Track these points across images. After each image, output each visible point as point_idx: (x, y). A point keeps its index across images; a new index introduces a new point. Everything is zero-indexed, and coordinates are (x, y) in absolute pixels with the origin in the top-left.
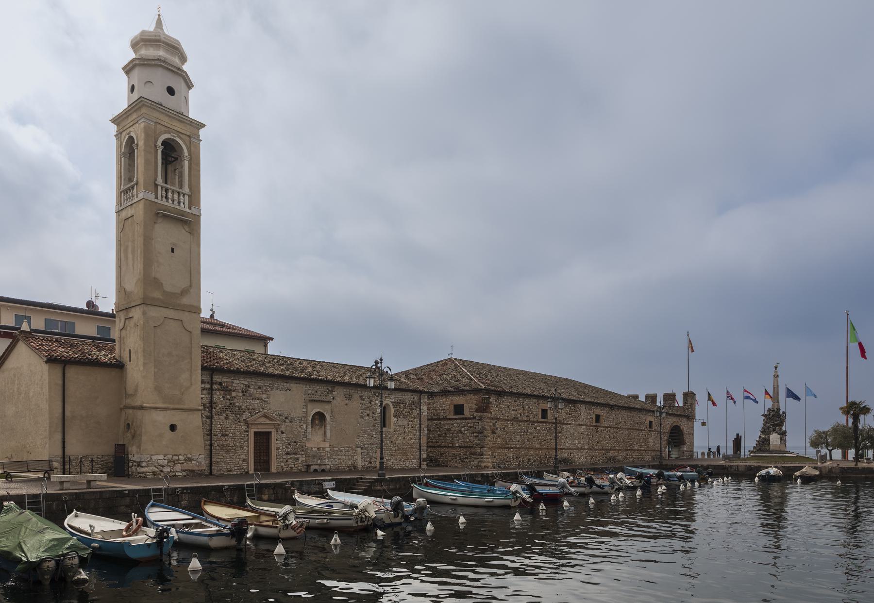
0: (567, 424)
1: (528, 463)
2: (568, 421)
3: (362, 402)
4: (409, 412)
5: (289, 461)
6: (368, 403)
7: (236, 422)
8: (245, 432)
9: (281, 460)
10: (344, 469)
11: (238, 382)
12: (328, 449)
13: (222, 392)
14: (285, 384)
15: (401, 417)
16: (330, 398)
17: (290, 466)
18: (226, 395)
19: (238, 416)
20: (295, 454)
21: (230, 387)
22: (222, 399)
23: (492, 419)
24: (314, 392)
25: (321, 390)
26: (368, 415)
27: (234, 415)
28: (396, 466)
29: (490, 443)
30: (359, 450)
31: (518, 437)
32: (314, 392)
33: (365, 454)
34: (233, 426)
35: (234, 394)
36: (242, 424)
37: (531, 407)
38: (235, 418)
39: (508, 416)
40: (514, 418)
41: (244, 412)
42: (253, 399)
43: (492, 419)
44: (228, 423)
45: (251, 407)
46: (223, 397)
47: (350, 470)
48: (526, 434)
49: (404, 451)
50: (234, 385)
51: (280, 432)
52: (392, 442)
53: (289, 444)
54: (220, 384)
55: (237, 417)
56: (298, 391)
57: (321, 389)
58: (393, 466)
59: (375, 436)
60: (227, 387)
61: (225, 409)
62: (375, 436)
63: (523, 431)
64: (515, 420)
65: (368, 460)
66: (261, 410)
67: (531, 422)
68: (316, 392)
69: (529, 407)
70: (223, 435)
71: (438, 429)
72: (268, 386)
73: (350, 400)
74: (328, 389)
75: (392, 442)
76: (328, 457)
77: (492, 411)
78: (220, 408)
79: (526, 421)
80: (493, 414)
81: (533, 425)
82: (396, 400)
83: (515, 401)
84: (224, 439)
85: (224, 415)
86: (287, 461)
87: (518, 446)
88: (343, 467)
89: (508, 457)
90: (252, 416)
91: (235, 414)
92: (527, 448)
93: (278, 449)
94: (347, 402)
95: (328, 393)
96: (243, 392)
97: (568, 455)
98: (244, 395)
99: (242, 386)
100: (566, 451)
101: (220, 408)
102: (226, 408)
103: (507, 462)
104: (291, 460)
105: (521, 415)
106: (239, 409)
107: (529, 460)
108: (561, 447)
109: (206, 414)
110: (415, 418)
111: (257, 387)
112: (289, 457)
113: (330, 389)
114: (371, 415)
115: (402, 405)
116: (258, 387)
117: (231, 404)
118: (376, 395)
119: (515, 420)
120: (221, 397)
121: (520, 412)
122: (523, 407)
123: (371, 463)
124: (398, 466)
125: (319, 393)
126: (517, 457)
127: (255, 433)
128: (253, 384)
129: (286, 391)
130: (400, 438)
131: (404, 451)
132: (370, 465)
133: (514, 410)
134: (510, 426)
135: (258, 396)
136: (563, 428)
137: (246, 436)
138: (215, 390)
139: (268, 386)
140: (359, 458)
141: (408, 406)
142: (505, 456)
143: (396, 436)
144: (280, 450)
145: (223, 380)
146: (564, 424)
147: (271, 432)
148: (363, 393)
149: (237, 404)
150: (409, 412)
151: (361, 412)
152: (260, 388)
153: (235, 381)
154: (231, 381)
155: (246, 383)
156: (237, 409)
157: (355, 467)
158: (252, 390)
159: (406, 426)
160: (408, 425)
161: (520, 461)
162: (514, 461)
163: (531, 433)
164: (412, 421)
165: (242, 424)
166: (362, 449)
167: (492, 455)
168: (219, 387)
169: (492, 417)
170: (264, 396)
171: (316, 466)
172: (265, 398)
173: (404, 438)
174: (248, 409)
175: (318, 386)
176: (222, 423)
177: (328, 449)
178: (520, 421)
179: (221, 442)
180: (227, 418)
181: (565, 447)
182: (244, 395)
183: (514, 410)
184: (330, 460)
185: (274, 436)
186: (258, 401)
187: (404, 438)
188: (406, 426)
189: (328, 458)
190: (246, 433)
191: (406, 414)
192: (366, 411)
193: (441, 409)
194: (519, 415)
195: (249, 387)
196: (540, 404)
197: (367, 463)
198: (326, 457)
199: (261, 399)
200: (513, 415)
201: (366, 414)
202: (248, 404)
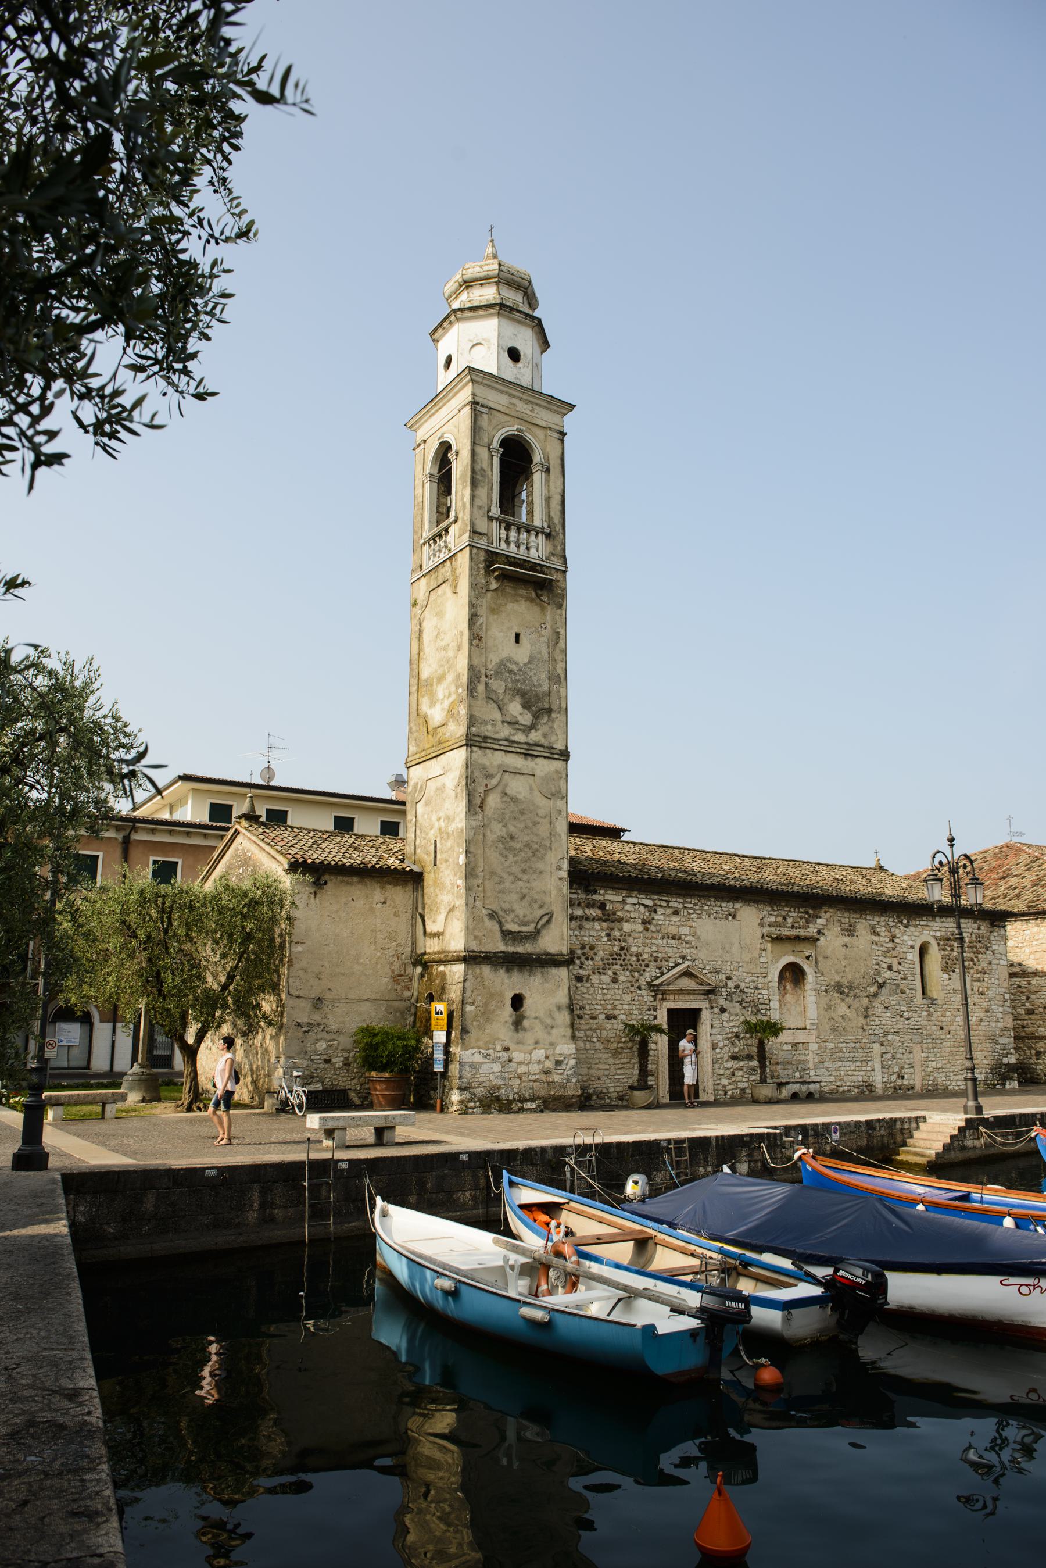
3: (875, 938)
4: (972, 960)
6: (887, 940)
7: (632, 989)
8: (649, 1010)
9: (722, 1072)
10: (849, 1091)
11: (635, 901)
12: (814, 1047)
13: (605, 924)
14: (724, 905)
16: (811, 931)
17: (740, 1085)
18: (612, 929)
19: (636, 974)
21: (619, 913)
22: (605, 939)
24: (780, 919)
25: (794, 914)
26: (890, 968)
27: (628, 973)
28: (954, 1083)
30: (876, 1046)
33: (889, 1056)
34: (627, 997)
35: (627, 927)
36: (644, 992)
38: (630, 979)
41: (647, 966)
42: (663, 938)
44: (617, 990)
45: (660, 955)
46: (608, 935)
47: (862, 1092)
50: (627, 908)
51: (716, 1010)
52: (942, 1028)
53: (737, 1036)
55: (633, 977)
59: (906, 1014)
60: (614, 913)
61: (611, 961)
62: (906, 1014)
65: (896, 1069)
66: (680, 961)
68: (785, 919)
70: (608, 1017)
71: (1024, 998)
72: (690, 908)
74: (807, 913)
75: (942, 1028)
76: (815, 1064)
78: (602, 959)
82: (943, 934)
84: (610, 1026)
85: (610, 973)
86: (733, 1074)
88: (846, 1088)
90: (662, 974)
91: (631, 971)
93: (714, 1047)
94: (846, 939)
95: (807, 922)
98: (647, 929)
99: (642, 909)
101: (602, 959)
102: (615, 957)
104: (741, 1073)
106: (638, 960)
109: (575, 972)
111: (669, 911)
112: (736, 1064)
113: (811, 912)
114: (895, 968)
116: (671, 910)
117: (622, 949)
118: (902, 923)
120: (603, 934)
123: (903, 1077)
125: (790, 920)
127: (670, 1011)
128: (664, 904)
129: (727, 918)
132: (899, 1082)
135: (673, 930)
137: (651, 1018)
138: (593, 919)
139: (690, 908)
140: (878, 1067)
143: (948, 1014)
144: (718, 1050)
145: (607, 897)
147: (700, 1010)
148: (877, 919)
149: (634, 949)
150: (972, 960)
152: (676, 913)
153: (630, 900)
154: (620, 899)
155: (650, 903)
156: (634, 959)
157: (870, 1087)
158: (662, 917)
165: (644, 992)
166: (882, 1045)
168: (599, 913)
170: (684, 931)
171: (795, 1086)
172: (686, 935)
174: (656, 961)
176: (605, 991)
177: (814, 1047)
179: (604, 1034)
180: (615, 980)
182: (647, 929)
184: (820, 1072)
185: (705, 1016)
186: (673, 941)
189: (816, 1067)
190: (652, 1012)
192: (886, 960)
193: (1027, 950)
195: (655, 911)
197: (895, 1077)
198: (811, 1066)
199: (680, 938)
201: (885, 966)
202: (654, 949)
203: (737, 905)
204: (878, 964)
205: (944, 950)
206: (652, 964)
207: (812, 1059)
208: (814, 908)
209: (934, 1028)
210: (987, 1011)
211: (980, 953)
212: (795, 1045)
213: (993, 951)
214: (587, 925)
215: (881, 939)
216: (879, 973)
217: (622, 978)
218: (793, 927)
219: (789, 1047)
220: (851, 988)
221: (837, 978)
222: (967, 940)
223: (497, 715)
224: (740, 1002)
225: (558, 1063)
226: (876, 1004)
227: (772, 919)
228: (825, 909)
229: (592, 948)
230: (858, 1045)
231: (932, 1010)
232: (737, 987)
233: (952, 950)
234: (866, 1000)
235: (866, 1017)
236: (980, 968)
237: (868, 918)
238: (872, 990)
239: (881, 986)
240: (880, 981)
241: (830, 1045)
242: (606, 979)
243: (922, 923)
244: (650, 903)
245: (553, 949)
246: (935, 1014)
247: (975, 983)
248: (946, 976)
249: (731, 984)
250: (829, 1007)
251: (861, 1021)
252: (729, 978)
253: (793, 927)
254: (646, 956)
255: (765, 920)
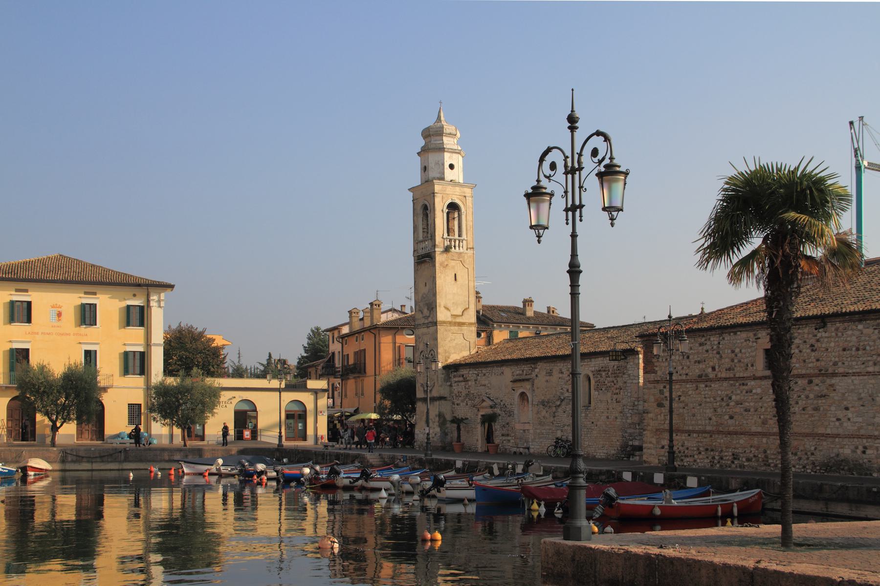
0: (845, 375)
1: (733, 462)
2: (851, 367)
3: (561, 375)
4: (613, 382)
5: (504, 442)
6: (566, 375)
15: (603, 389)
20: (508, 435)
23: (657, 382)
24: (521, 372)
29: (652, 423)
31: (708, 411)
32: (521, 372)
37: (737, 350)
39: (687, 374)
40: (700, 376)
43: (657, 382)
48: (728, 405)
49: (608, 435)
50: (470, 375)
54: (463, 376)
56: (509, 373)
57: (526, 368)
58: (595, 454)
63: (719, 399)
64: (702, 378)
67: (736, 379)
69: (733, 352)
73: (551, 375)
75: (593, 423)
77: (656, 369)
79: (726, 379)
80: (659, 373)
81: (743, 384)
83: (701, 345)
87: (708, 428)
89: (687, 449)
92: (729, 433)
94: (548, 378)
96: (475, 380)
97: (854, 452)
100: (846, 441)
102: (467, 395)
103: (686, 456)
105: (714, 369)
107: (735, 457)
108: (829, 431)
110: (621, 389)
113: (533, 366)
115: (604, 374)
119: (702, 378)
121: (711, 364)
122: (718, 353)
124: (601, 454)
125: (525, 372)
126: (707, 450)
130: (602, 418)
131: (608, 435)
133: (699, 362)
134: (690, 393)
135: (483, 383)
136: (832, 385)
141: (612, 374)
142: (682, 446)
143: (597, 415)
146: (834, 375)
150: (613, 382)
151: (560, 388)
153: (470, 372)
155: (476, 372)
159: (609, 401)
160: (612, 400)
161: (713, 458)
162: (701, 456)
163: (739, 403)
164: (617, 394)
167: (658, 442)
169: (659, 379)
170: (487, 382)
173: (608, 417)
175: (523, 364)
177: (531, 431)
178: (711, 380)
180: (467, 404)
181: (841, 431)
183: (699, 362)
187: (608, 417)
188: (609, 401)
191: (609, 384)
194: (710, 370)
196: (759, 341)
200: (696, 370)
201: (565, 390)
203: (504, 368)
204: (562, 389)
205: (597, 377)
206: (477, 397)
207: (531, 437)
208: (534, 364)
209: (588, 423)
210: (621, 412)
211: (618, 377)
212: (524, 431)
213: (629, 375)
214: (460, 384)
215: (564, 375)
216: (562, 393)
217: (469, 404)
218: (526, 375)
219: (522, 431)
220: (548, 402)
221: (543, 398)
222: (611, 370)
223: (421, 316)
224: (504, 411)
225: (435, 434)
226: (560, 410)
227: (518, 372)
228: (539, 364)
229: (461, 392)
230: (550, 431)
231: (588, 413)
232: (504, 405)
233: (601, 377)
234: (554, 409)
235: (554, 417)
236: (618, 386)
237: (558, 365)
238: (558, 403)
239: (562, 401)
240: (562, 398)
241: (538, 431)
242: (464, 404)
243: (585, 363)
244: (476, 372)
245: (435, 396)
246: (589, 415)
247: (615, 396)
248: (597, 393)
249: (502, 404)
250: (538, 413)
251: (552, 419)
252: (501, 401)
253: (526, 375)
254: (475, 394)
255: (515, 373)
